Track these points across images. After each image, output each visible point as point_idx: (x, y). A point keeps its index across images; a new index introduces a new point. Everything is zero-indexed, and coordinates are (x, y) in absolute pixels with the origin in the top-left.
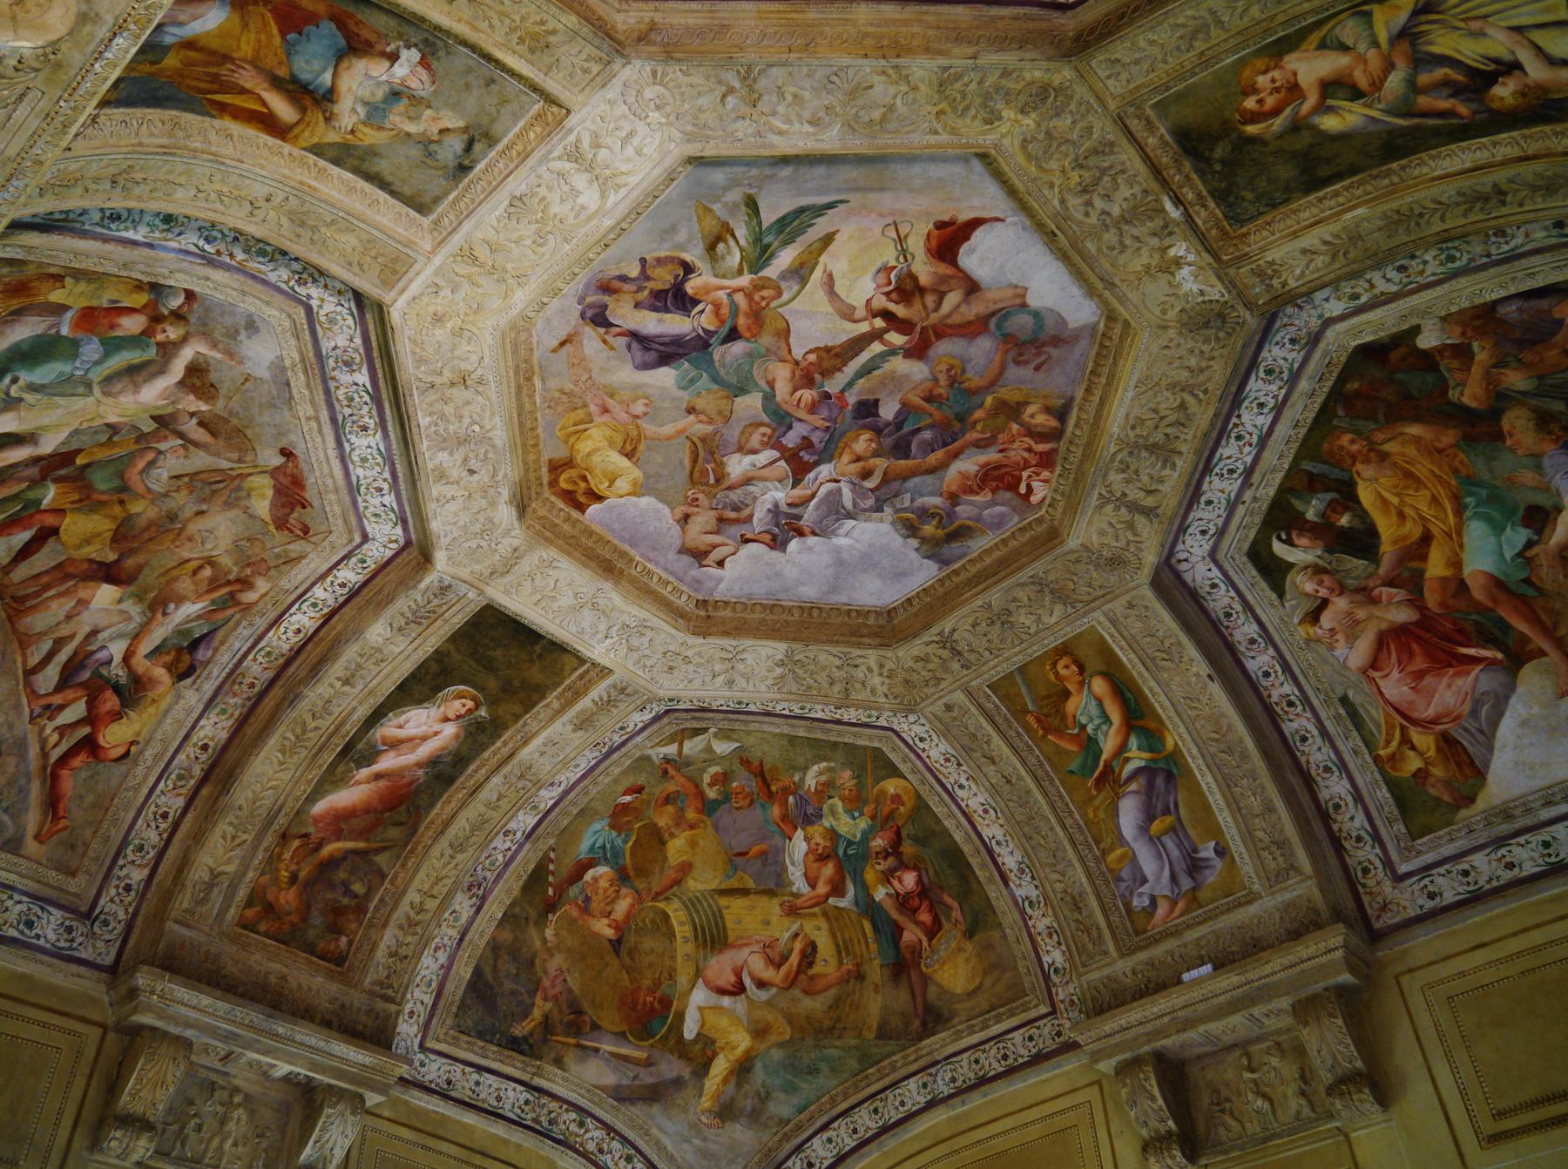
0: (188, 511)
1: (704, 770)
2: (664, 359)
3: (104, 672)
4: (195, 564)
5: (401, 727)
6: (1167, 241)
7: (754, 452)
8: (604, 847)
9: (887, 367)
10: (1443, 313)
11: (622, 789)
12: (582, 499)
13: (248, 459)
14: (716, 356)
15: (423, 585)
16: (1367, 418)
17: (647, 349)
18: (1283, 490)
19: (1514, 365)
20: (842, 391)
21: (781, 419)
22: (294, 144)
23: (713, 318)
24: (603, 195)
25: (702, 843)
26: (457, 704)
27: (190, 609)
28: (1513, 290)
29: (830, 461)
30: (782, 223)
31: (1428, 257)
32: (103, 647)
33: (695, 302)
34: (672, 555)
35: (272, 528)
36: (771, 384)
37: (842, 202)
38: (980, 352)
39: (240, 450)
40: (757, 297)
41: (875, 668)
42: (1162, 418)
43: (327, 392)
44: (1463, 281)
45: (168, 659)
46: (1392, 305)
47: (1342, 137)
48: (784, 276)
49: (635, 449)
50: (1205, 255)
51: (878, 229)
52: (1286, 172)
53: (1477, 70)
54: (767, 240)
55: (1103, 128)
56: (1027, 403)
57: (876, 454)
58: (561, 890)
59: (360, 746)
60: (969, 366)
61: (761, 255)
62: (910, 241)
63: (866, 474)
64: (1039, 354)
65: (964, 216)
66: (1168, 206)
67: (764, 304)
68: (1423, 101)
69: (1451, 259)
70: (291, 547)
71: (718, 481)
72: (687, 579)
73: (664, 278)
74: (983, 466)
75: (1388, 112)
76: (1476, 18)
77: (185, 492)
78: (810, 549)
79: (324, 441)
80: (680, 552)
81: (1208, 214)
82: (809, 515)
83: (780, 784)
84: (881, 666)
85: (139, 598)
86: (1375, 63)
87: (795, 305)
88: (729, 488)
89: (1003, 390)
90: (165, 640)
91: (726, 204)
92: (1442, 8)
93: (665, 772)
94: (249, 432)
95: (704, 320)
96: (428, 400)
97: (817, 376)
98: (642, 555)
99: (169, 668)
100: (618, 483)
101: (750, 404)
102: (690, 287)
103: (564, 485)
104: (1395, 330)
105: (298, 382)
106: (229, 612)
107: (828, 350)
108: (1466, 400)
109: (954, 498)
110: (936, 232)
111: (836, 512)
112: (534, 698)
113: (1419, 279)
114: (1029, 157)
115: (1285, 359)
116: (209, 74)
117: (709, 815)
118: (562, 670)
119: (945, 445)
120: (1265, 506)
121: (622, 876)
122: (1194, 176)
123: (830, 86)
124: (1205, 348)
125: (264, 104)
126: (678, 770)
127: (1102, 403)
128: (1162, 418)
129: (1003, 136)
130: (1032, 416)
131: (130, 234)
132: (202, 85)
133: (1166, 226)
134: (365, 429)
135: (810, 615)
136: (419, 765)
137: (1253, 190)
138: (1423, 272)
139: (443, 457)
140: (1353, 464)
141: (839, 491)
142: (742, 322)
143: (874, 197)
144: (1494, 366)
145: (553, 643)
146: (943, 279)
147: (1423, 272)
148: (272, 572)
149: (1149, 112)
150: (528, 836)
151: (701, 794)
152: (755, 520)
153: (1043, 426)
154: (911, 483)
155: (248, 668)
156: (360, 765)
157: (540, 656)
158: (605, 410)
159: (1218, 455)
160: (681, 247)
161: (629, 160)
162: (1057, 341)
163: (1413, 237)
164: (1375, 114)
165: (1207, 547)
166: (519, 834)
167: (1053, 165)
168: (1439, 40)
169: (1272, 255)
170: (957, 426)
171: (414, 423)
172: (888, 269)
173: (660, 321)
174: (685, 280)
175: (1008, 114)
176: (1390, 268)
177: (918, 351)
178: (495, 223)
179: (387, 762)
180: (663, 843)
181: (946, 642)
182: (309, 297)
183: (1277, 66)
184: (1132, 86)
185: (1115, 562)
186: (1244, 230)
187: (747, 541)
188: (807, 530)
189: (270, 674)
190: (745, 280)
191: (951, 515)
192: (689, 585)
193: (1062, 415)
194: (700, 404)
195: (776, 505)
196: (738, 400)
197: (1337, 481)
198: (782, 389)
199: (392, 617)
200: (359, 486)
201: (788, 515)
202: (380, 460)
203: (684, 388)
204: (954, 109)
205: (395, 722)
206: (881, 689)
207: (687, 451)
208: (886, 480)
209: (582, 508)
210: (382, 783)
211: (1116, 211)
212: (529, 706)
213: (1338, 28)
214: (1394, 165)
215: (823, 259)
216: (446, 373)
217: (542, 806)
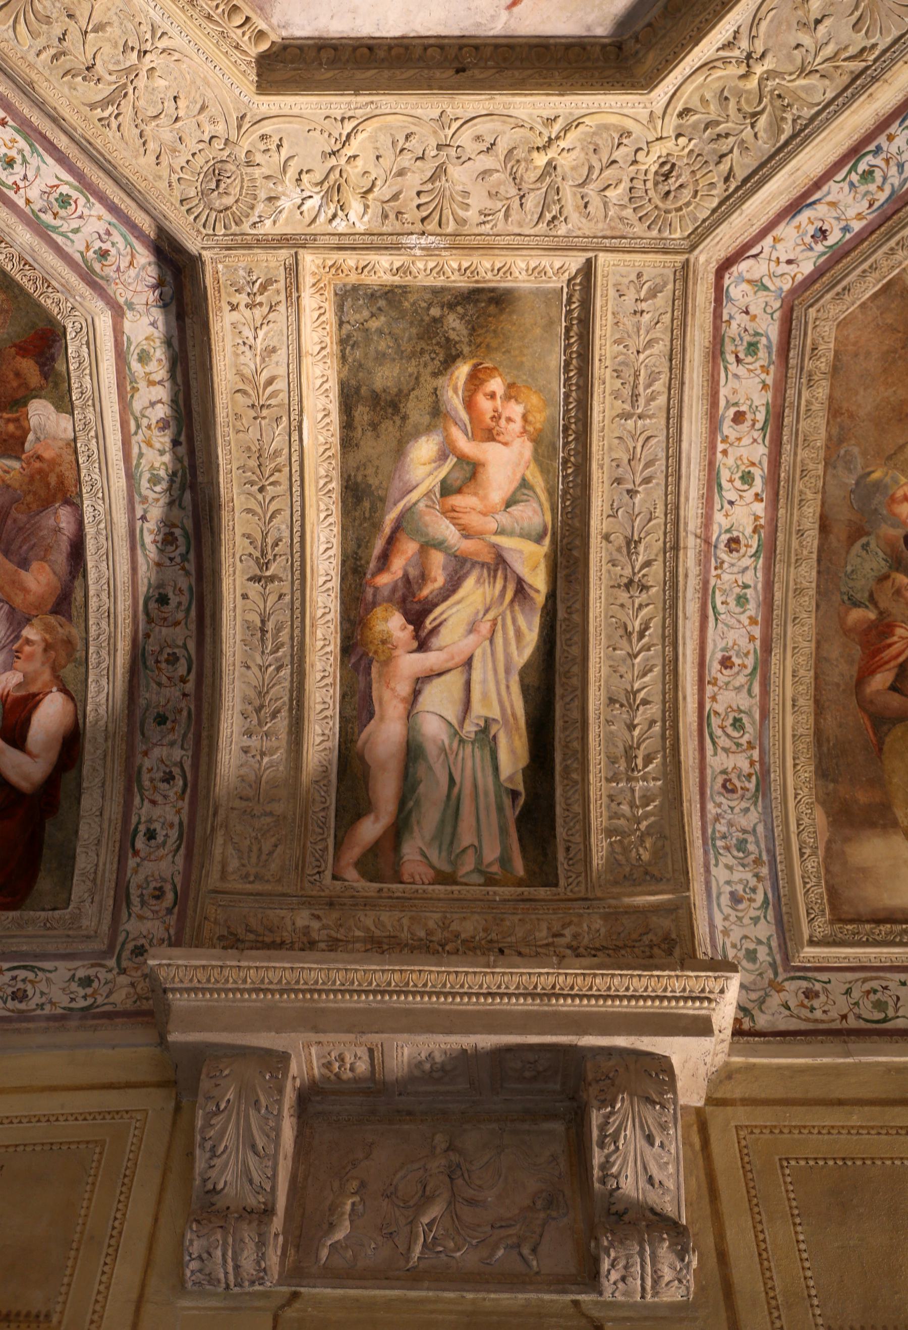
6: (375, 209)
28: (90, 531)
47: (400, 451)
53: (430, 611)
68: (409, 548)
75: (409, 510)
76: (493, 632)
86: (475, 521)
92: (517, 608)
113: (140, 437)
137: (380, 332)
138: (149, 444)
147: (149, 444)
164: (414, 496)
168: (480, 591)
183: (525, 431)
186: (329, 294)
213: (535, 505)
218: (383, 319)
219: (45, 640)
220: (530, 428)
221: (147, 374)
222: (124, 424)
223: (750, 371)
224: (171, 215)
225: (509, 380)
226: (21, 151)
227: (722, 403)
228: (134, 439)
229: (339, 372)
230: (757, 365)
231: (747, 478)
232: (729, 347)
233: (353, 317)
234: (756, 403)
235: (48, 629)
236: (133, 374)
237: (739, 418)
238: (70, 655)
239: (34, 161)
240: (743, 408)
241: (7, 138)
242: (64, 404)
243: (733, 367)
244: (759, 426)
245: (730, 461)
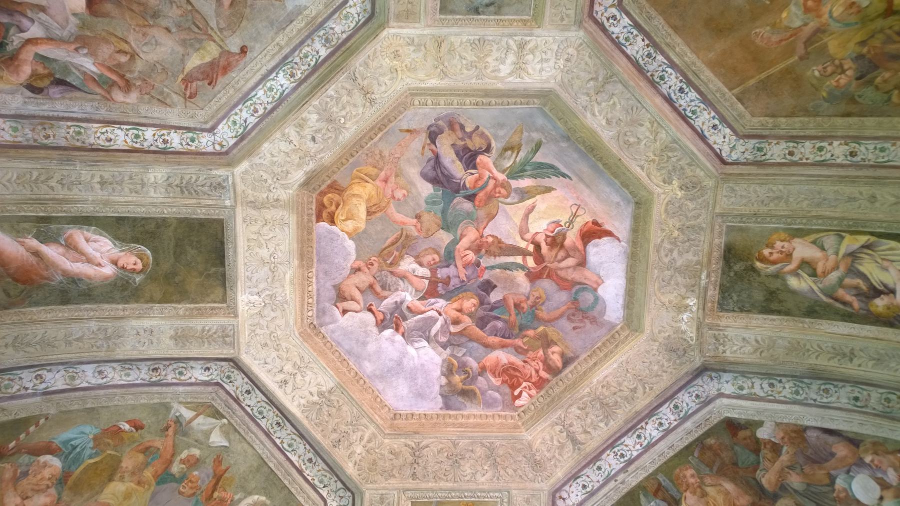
0: (165, 23)
1: (188, 446)
2: (435, 181)
3: (12, 31)
4: (126, 47)
5: (87, 240)
6: (689, 294)
7: (421, 265)
8: (74, 448)
9: (515, 273)
10: (779, 421)
11: (131, 416)
12: (325, 215)
13: (225, 33)
14: (455, 201)
15: (215, 172)
16: (707, 466)
17: (434, 169)
18: (641, 487)
19: (798, 470)
20: (486, 268)
21: (449, 257)
23: (473, 181)
24: (510, 74)
25: (134, 499)
26: (134, 259)
27: (88, 64)
28: (819, 424)
29: (447, 300)
30: (541, 166)
31: (787, 386)
32: (33, 21)
33: (475, 167)
34: (329, 284)
35: (181, 76)
36: (462, 236)
37: (570, 178)
38: (561, 298)
39: (229, 25)
40: (497, 190)
41: (366, 438)
42: (621, 390)
43: (302, 43)
44: (797, 408)
45: (41, 70)
46: (755, 403)
47: (794, 292)
48: (517, 190)
49: (375, 213)
50: (700, 311)
51: (571, 203)
52: (759, 296)
54: (528, 168)
55: (703, 219)
56: (556, 344)
57: (470, 315)
58: (18, 451)
59: (53, 226)
60: (547, 303)
61: (517, 173)
62: (578, 219)
63: (456, 322)
64: (582, 321)
65: (607, 227)
66: (704, 276)
67: (497, 195)
69: (797, 393)
70: (174, 96)
71: (391, 264)
72: (321, 306)
73: (476, 143)
74: (510, 363)
77: (179, 12)
78: (393, 341)
79: (269, 61)
80: (334, 286)
81: (713, 293)
82: (412, 321)
83: (223, 494)
84: (369, 441)
85: (83, 25)
87: (508, 207)
88: (392, 273)
89: (551, 328)
90: (55, 60)
91: (530, 136)
93: (167, 429)
94: (244, 23)
95: (468, 179)
96: (344, 84)
97: (484, 250)
98: (317, 271)
99: (34, 75)
100: (349, 222)
101: (444, 238)
102: (481, 158)
103: (325, 200)
104: (751, 418)
105: (299, 24)
106: (98, 90)
107: (500, 242)
108: (764, 481)
109: (483, 369)
110: (591, 224)
111: (423, 332)
112: (174, 298)
113: (777, 396)
114: (666, 210)
115: (688, 405)
117: (158, 483)
118: (208, 295)
119: (503, 337)
120: (626, 490)
121: (62, 480)
122: (720, 271)
123: (630, 111)
124: (666, 364)
126: (175, 434)
127: (595, 364)
128: (621, 390)
129: (664, 193)
130: (553, 353)
133: (693, 286)
134: (292, 75)
135: (358, 381)
136: (65, 273)
137: (738, 296)
138: (780, 392)
139: (314, 117)
140: (686, 491)
141: (437, 320)
142: (481, 195)
143: (582, 186)
144: (788, 467)
145: (224, 275)
146: (575, 249)
147: (780, 392)
148: (146, 97)
149: (724, 228)
150: (46, 393)
151: (170, 462)
152: (385, 302)
153: (554, 362)
154: (471, 344)
155: (59, 127)
156: (37, 237)
157: (208, 276)
158: (386, 181)
159: (622, 440)
160: (496, 137)
161: (534, 70)
162: (594, 321)
163: (797, 361)
165: (580, 499)
166: (43, 386)
167: (671, 222)
169: (729, 333)
170: (516, 331)
171: (327, 86)
172: (557, 224)
173: (453, 161)
174: (481, 153)
175: (676, 183)
176: (766, 381)
177: (533, 277)
178: (464, 40)
179: (52, 252)
180: (110, 480)
181: (416, 453)
183: (789, 241)
184: (731, 207)
185: (537, 465)
186: (721, 314)
187: (370, 310)
188: (402, 330)
189: (63, 143)
190: (501, 177)
191: (473, 380)
192: (318, 310)
193: (567, 362)
194: (426, 217)
195: (402, 303)
196: (442, 231)
197: (672, 497)
198: (465, 243)
199: (175, 174)
200: (251, 99)
201: (402, 312)
202: (277, 97)
203: (427, 203)
204: (659, 164)
205: (88, 234)
206: (357, 458)
207: (395, 236)
208: (461, 333)
209: (319, 218)
210: (33, 259)
211: (679, 263)
212: (165, 300)
214: (807, 320)
215: (538, 197)
216: (366, 82)
217: (77, 382)
218: (733, 294)
219: (872, 454)
220: (788, 239)
221: (748, 388)
222: (770, 401)
223: (770, 150)
224: (686, 370)
225: (764, 246)
226: (657, 419)
227: (784, 161)
228: (777, 398)
229: (755, 314)
230: (767, 147)
231: (821, 149)
232: (759, 159)
233: (731, 307)
234: (785, 147)
235: (866, 451)
236: (748, 394)
237: (791, 154)
238: (881, 444)
239: (661, 415)
240: (787, 152)
241: (652, 423)
242: (760, 424)
243: (767, 157)
244: (796, 145)
245: (811, 156)
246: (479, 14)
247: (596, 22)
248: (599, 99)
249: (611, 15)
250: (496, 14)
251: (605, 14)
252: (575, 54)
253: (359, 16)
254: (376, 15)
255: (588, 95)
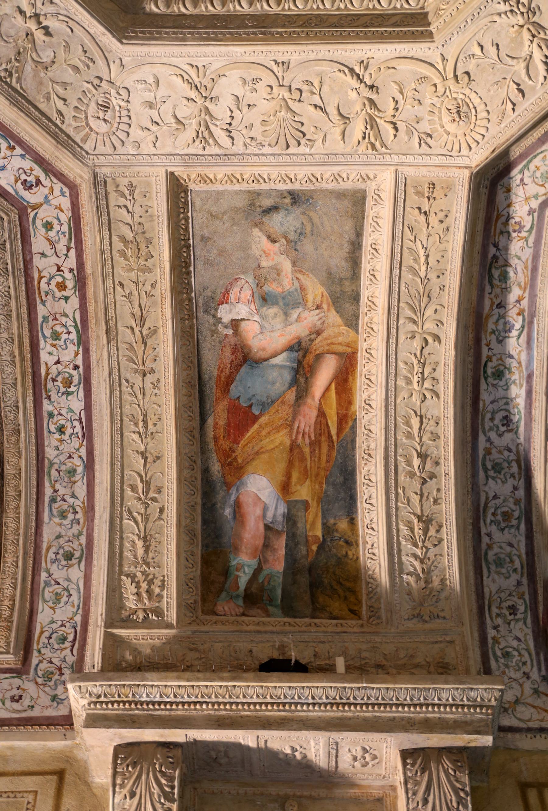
22: (356, 342)
116: (312, 452)
125: (328, 389)
131: (521, 402)
132: (324, 450)
182: (531, 212)
246: (291, 193)
247: (61, 177)
248: (20, 19)
249: (35, 190)
250: (258, 194)
251: (46, 191)
252: (91, 121)
253: (522, 180)
254: (487, 183)
255: (47, 32)
